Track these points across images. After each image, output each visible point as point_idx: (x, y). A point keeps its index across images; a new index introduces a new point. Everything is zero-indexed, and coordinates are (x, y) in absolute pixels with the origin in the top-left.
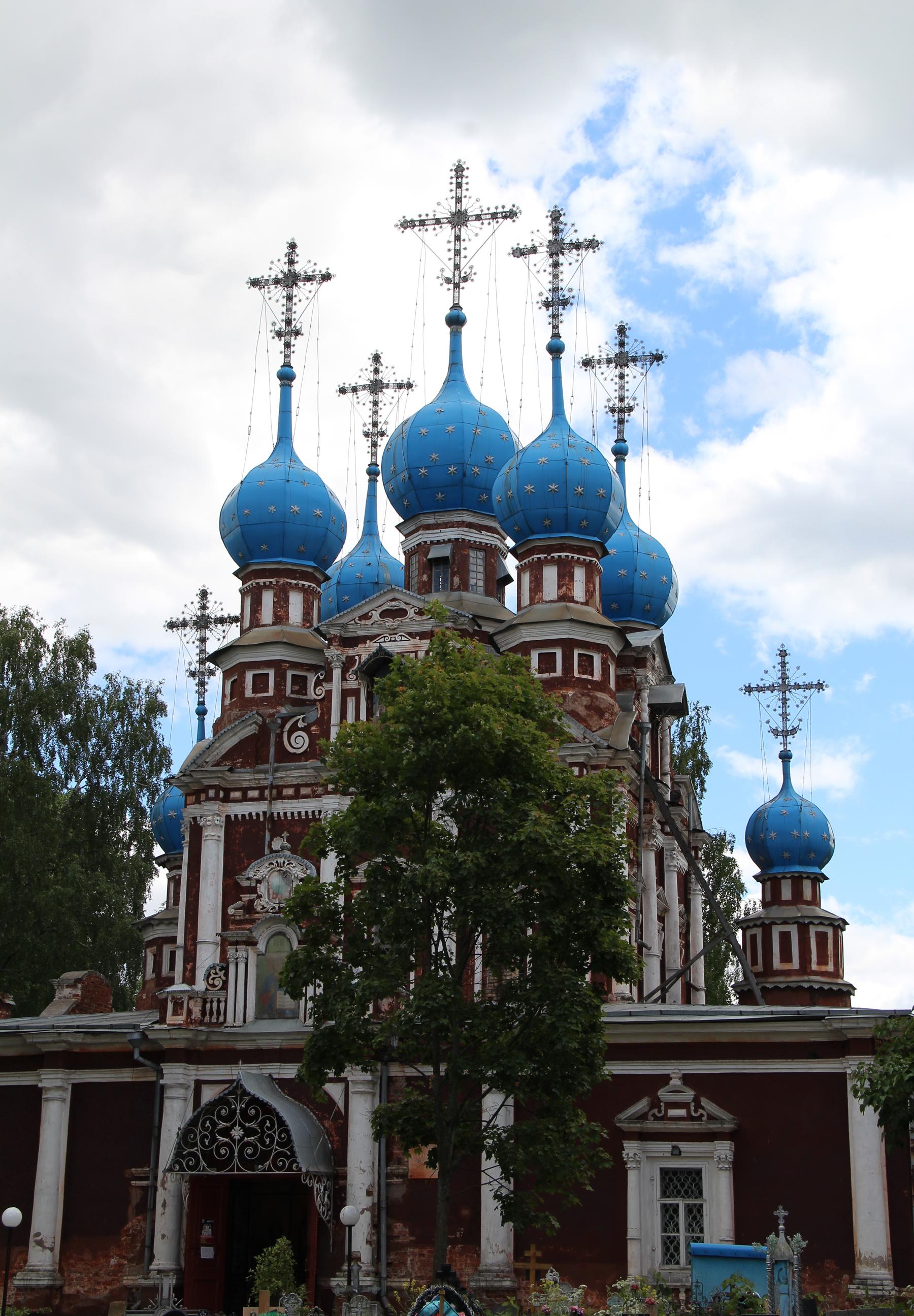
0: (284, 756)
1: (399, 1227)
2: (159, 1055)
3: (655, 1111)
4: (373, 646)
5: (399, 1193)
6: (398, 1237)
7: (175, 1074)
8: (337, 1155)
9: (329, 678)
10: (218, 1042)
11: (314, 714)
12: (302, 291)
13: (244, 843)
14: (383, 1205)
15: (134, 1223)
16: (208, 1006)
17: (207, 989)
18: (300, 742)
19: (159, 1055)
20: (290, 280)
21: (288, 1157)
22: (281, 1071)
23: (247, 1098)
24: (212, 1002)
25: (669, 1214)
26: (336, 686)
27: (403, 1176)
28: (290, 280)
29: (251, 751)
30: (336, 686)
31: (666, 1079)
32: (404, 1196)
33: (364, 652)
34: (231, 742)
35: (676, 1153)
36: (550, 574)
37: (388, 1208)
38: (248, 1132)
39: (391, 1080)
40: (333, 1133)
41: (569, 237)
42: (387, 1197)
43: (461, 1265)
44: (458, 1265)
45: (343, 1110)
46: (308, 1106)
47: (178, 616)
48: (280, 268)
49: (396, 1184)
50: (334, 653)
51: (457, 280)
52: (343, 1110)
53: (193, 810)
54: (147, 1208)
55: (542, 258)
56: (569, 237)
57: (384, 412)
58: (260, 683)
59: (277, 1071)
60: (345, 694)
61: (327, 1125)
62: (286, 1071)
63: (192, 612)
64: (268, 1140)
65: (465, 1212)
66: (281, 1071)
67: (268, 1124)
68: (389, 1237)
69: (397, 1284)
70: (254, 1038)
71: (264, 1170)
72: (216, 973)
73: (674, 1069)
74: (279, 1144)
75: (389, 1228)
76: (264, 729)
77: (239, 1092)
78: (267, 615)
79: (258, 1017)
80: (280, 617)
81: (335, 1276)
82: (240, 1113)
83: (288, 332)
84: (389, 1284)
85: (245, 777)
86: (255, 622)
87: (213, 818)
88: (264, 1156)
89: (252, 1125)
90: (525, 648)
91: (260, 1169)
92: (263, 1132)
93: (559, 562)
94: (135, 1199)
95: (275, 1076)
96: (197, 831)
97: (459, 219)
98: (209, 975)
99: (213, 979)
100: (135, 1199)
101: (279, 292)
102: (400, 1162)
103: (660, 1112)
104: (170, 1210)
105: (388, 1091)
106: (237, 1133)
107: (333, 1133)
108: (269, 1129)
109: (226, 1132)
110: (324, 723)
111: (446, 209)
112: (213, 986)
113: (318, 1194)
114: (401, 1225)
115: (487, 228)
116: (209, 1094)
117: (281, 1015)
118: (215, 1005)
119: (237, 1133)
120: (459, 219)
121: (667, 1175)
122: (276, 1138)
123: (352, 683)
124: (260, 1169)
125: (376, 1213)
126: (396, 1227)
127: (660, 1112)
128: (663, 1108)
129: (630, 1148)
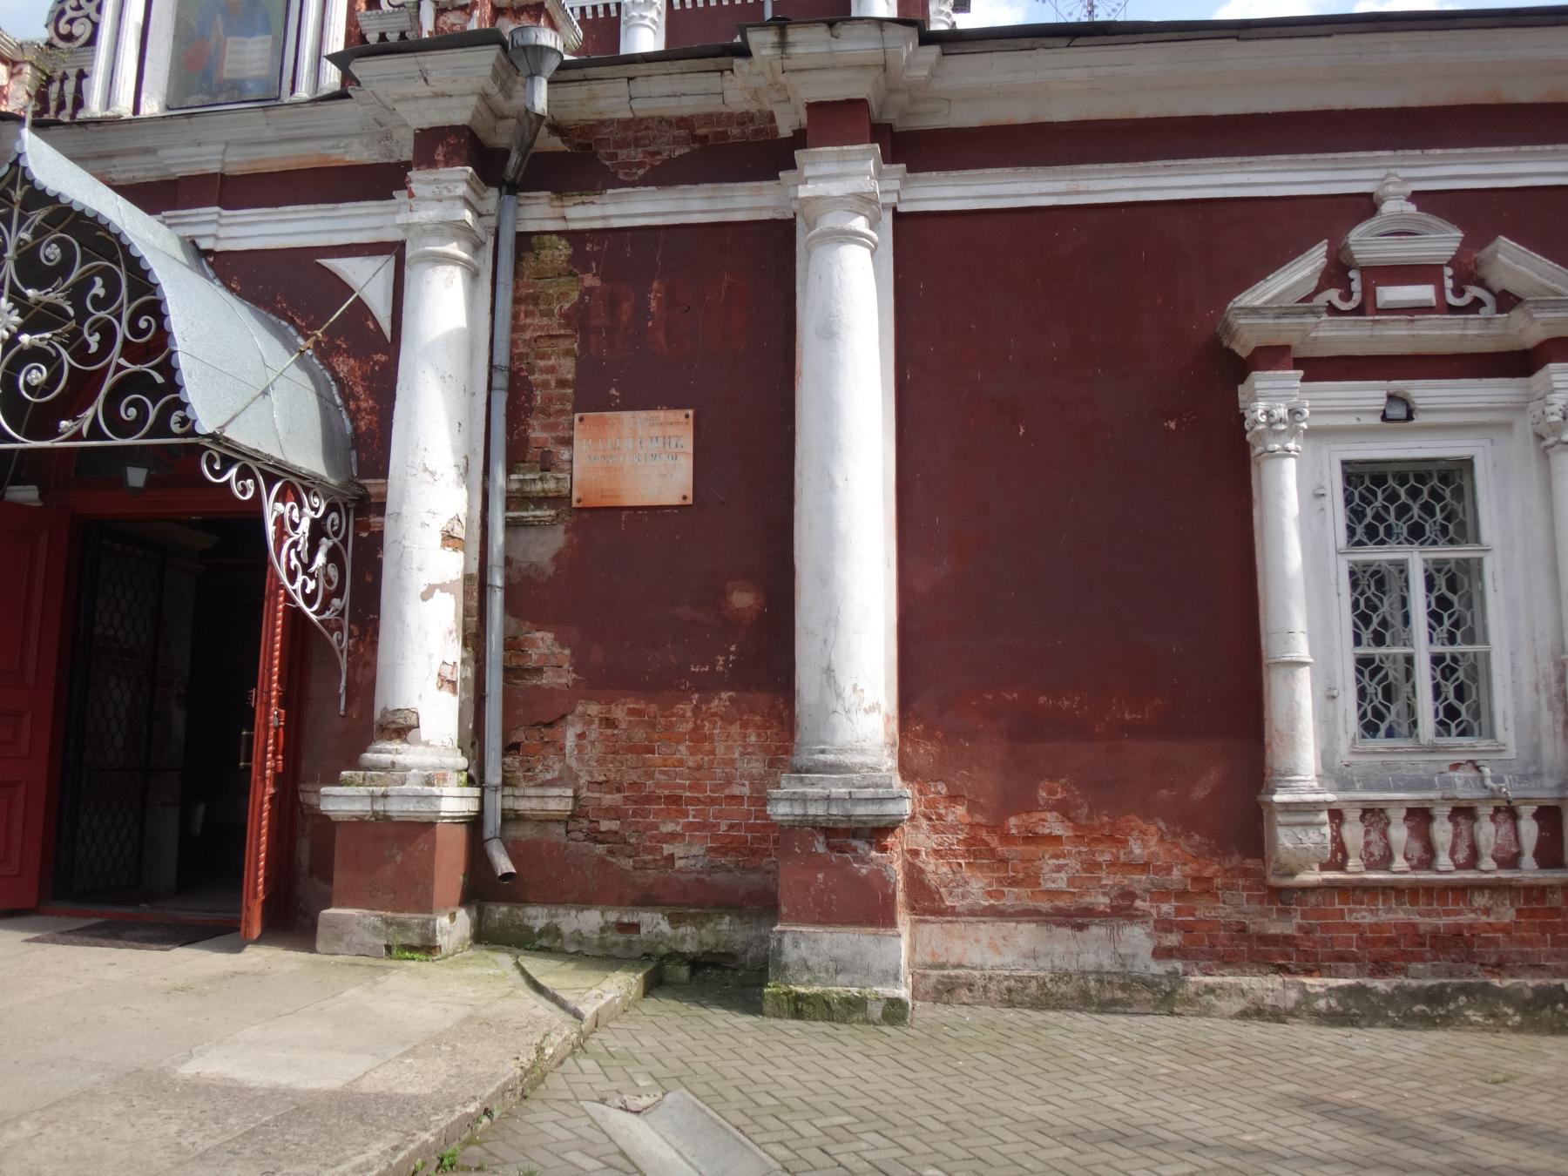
1: (542, 643)
3: (1333, 295)
5: (545, 547)
6: (538, 671)
14: (497, 579)
16: (54, 89)
17: (50, 44)
21: (155, 392)
22: (223, 233)
23: (38, 216)
24: (64, 77)
25: (1373, 598)
27: (557, 500)
31: (1364, 206)
32: (557, 558)
35: (1401, 414)
37: (508, 589)
39: (524, 242)
40: (359, 389)
42: (508, 561)
43: (729, 749)
44: (720, 749)
45: (387, 327)
46: (292, 322)
49: (539, 524)
52: (387, 327)
59: (210, 229)
61: (343, 370)
62: (235, 231)
64: (94, 341)
65: (742, 599)
66: (223, 233)
67: (99, 289)
68: (509, 672)
69: (535, 804)
70: (149, 142)
71: (77, 436)
72: (79, 8)
73: (1391, 177)
74: (129, 351)
75: (512, 645)
77: (18, 195)
81: (336, 781)
82: (17, 264)
84: (510, 803)
89: (54, 296)
92: (82, 315)
95: (205, 244)
98: (62, 13)
99: (71, 22)
102: (547, 464)
103: (1347, 296)
105: (517, 273)
107: (359, 389)
108: (99, 303)
112: (69, 37)
113: (281, 534)
114: (549, 636)
118: (70, 87)
121: (1363, 482)
122: (122, 331)
125: (474, 604)
126: (533, 643)
127: (1347, 296)
128: (1356, 286)
129: (1271, 397)
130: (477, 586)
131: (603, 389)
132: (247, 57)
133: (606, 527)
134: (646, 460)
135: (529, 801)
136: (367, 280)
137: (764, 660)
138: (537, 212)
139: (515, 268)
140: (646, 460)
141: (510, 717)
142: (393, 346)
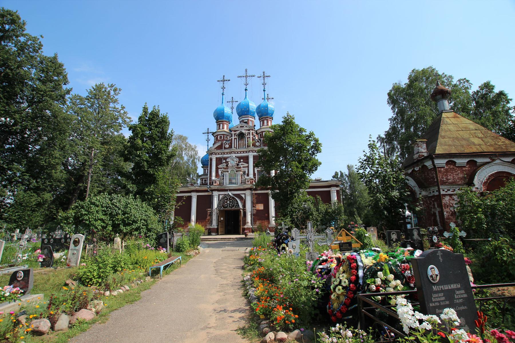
0: (225, 148)
2: (212, 190)
4: (239, 132)
5: (255, 212)
7: (216, 194)
8: (244, 206)
9: (232, 136)
10: (222, 188)
11: (229, 142)
12: (225, 82)
13: (219, 161)
15: (208, 218)
18: (227, 146)
19: (212, 190)
20: (224, 81)
26: (233, 138)
28: (224, 81)
29: (220, 147)
30: (233, 138)
33: (237, 132)
34: (216, 146)
36: (265, 122)
38: (230, 202)
41: (266, 75)
47: (204, 132)
48: (222, 79)
50: (233, 133)
51: (246, 85)
53: (210, 156)
54: (211, 215)
55: (262, 78)
56: (266, 75)
57: (234, 105)
58: (221, 137)
60: (234, 139)
63: (206, 131)
76: (222, 144)
78: (221, 127)
79: (229, 184)
80: (223, 128)
83: (223, 88)
85: (219, 151)
86: (219, 129)
87: (214, 158)
88: (233, 206)
90: (262, 132)
91: (233, 208)
93: (267, 120)
94: (209, 214)
96: (211, 159)
97: (246, 77)
100: (209, 214)
101: (222, 82)
104: (215, 216)
106: (228, 202)
109: (226, 202)
110: (231, 143)
111: (245, 75)
115: (251, 78)
116: (221, 197)
117: (233, 183)
119: (228, 202)
120: (246, 77)
123: (236, 137)
124: (233, 208)
130: (251, 214)
131: (258, 202)
132: (234, 181)
133: (258, 211)
134: (260, 207)
135: (255, 227)
136: (243, 196)
137: (268, 218)
138: (254, 192)
139: (252, 195)
140: (260, 207)
141: (253, 221)
142: (245, 200)
